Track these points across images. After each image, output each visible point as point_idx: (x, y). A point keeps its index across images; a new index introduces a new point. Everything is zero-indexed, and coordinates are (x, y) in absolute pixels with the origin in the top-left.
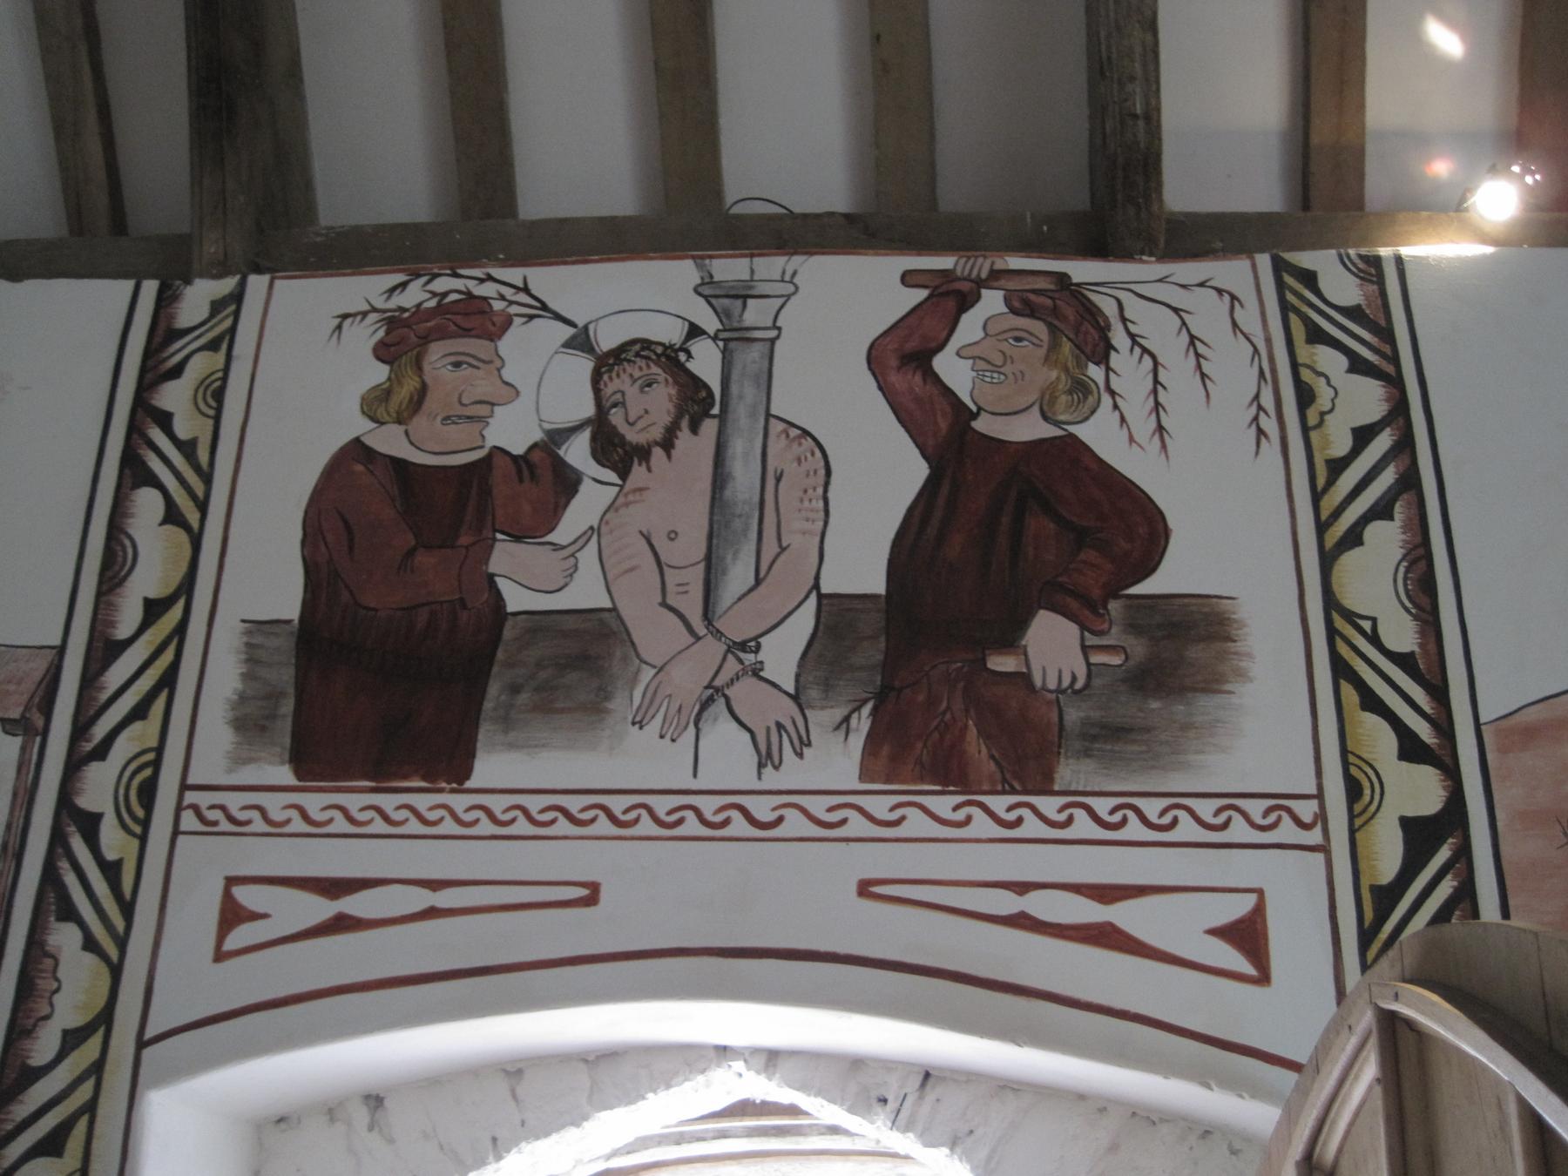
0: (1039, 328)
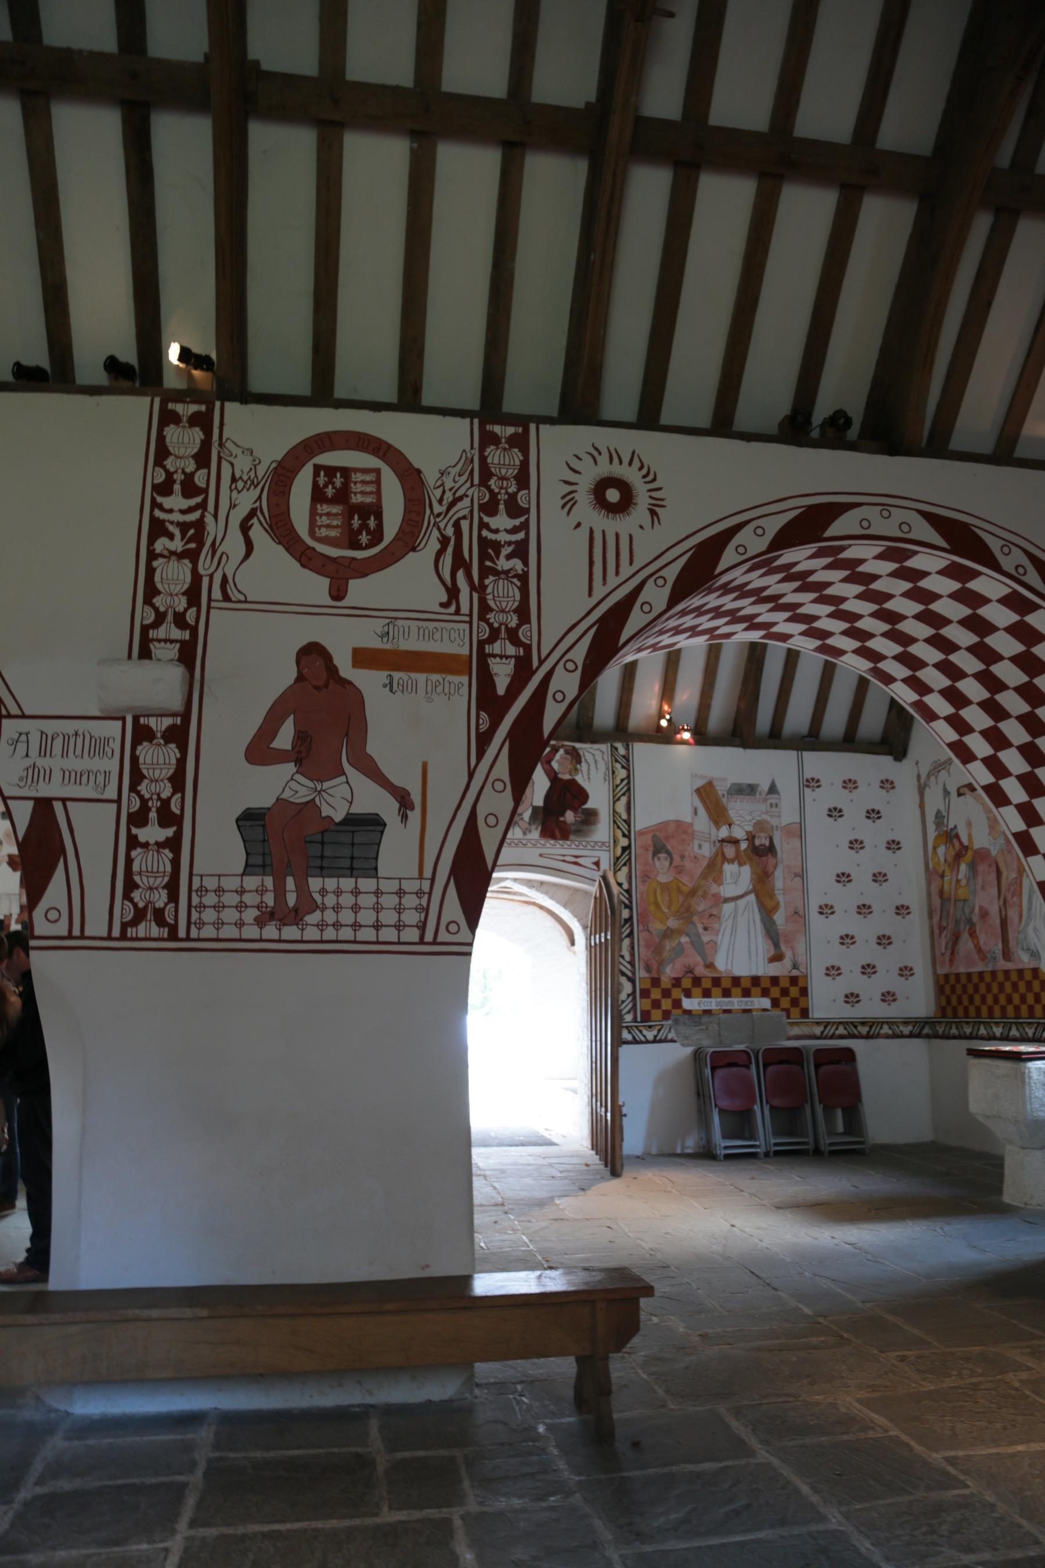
0: (569, 757)
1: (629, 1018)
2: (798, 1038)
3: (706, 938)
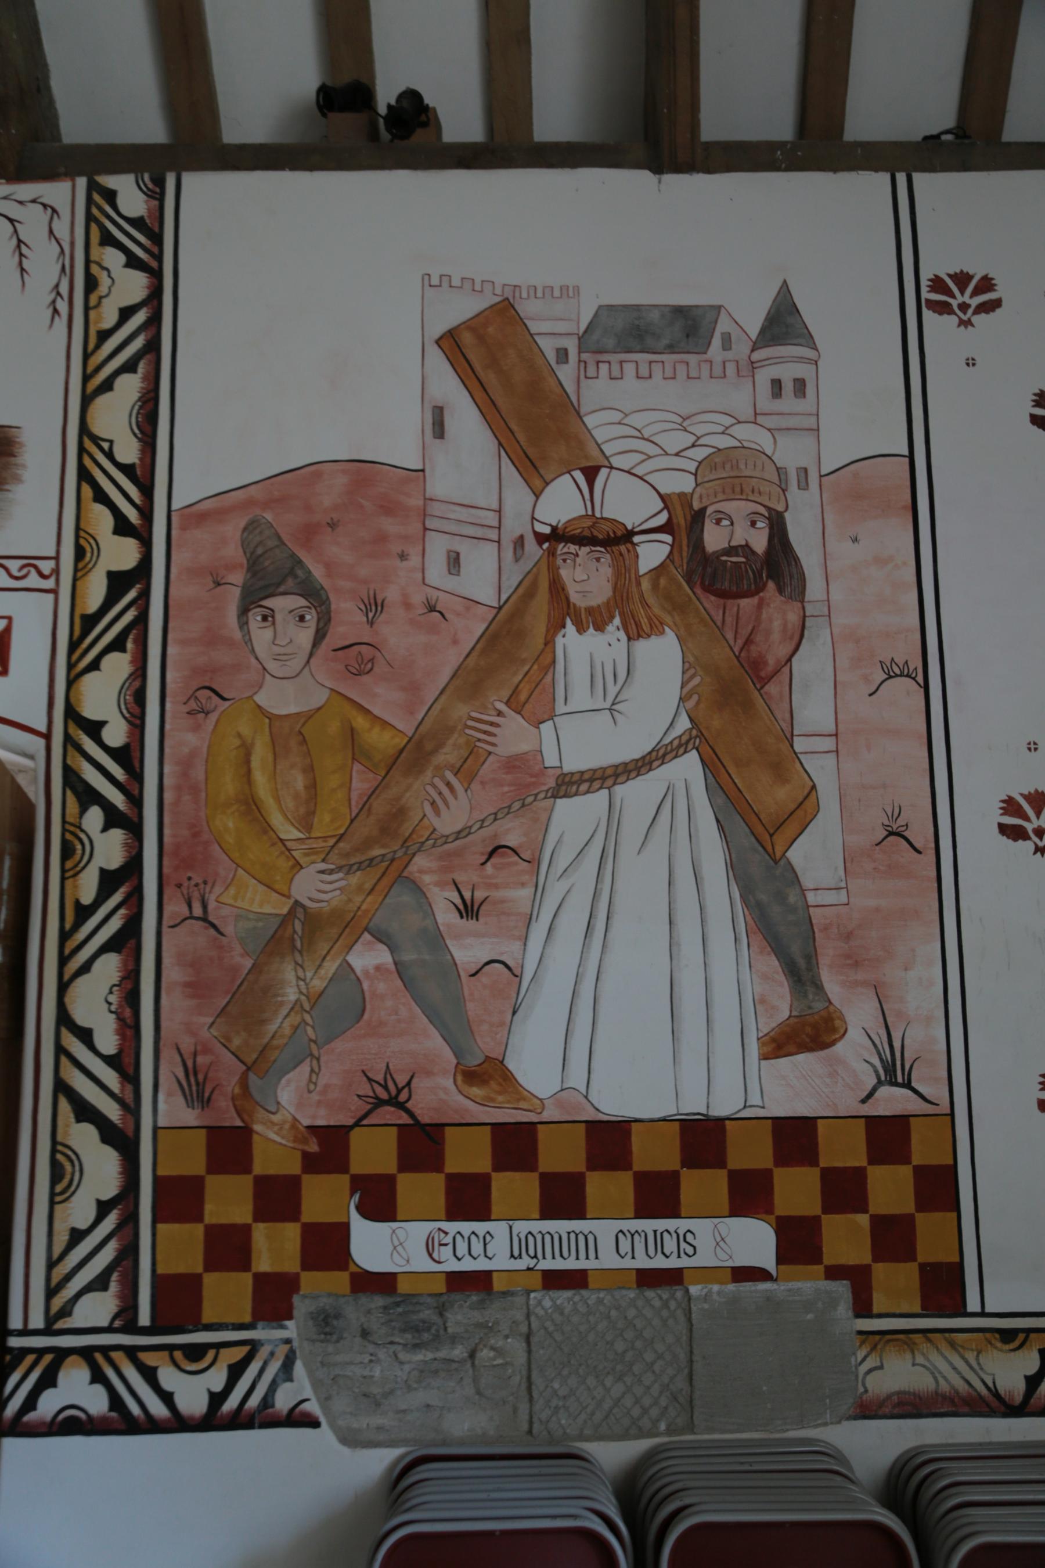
1: (97, 1309)
2: (910, 1406)
3: (469, 950)
